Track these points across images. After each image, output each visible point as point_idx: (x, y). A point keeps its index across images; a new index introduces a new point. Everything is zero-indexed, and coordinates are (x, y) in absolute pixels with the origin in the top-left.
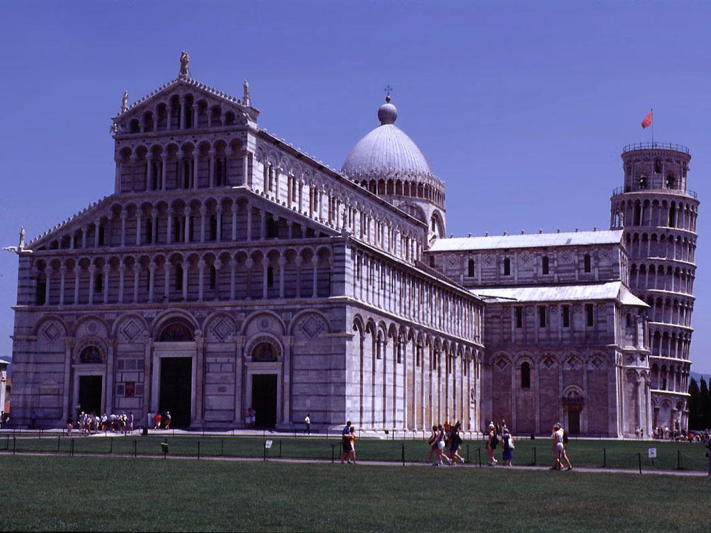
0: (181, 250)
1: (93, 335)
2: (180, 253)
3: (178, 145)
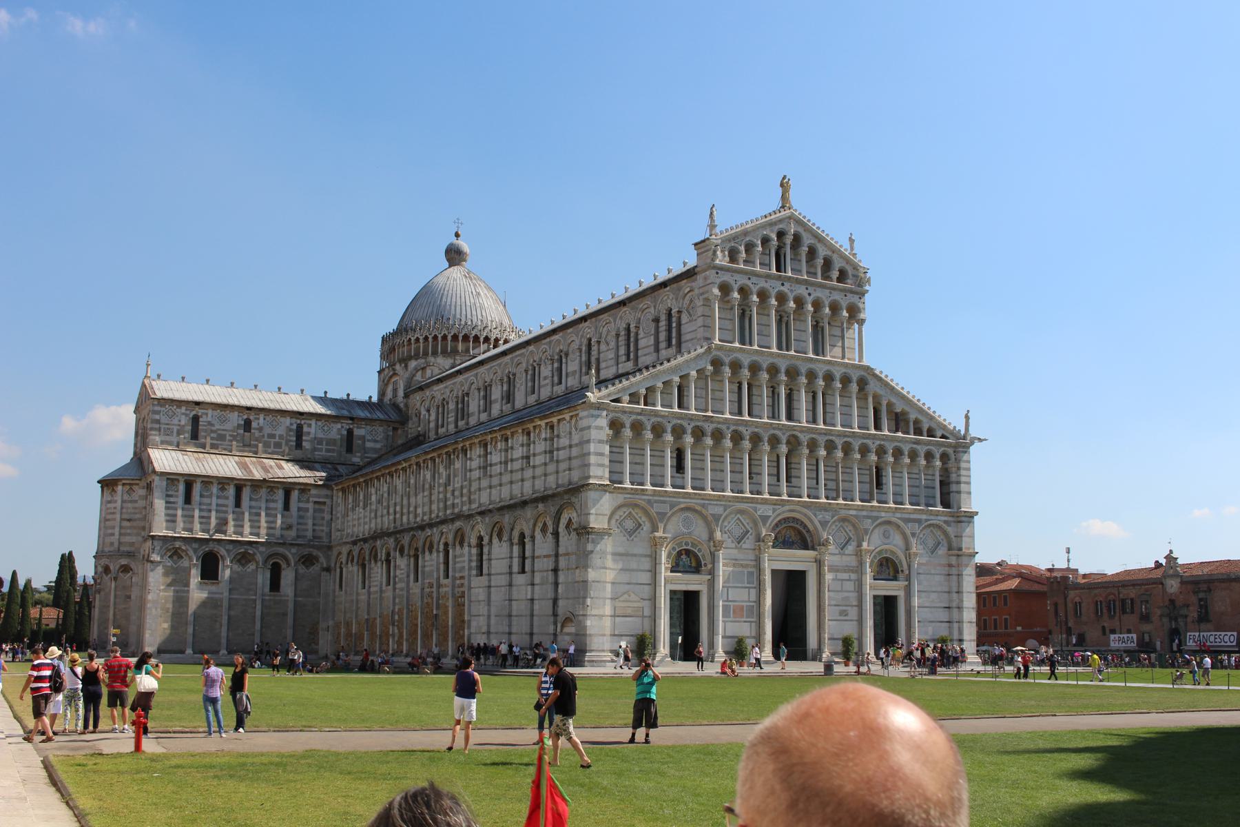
0: (801, 432)
1: (690, 533)
2: (799, 435)
3: (789, 294)
